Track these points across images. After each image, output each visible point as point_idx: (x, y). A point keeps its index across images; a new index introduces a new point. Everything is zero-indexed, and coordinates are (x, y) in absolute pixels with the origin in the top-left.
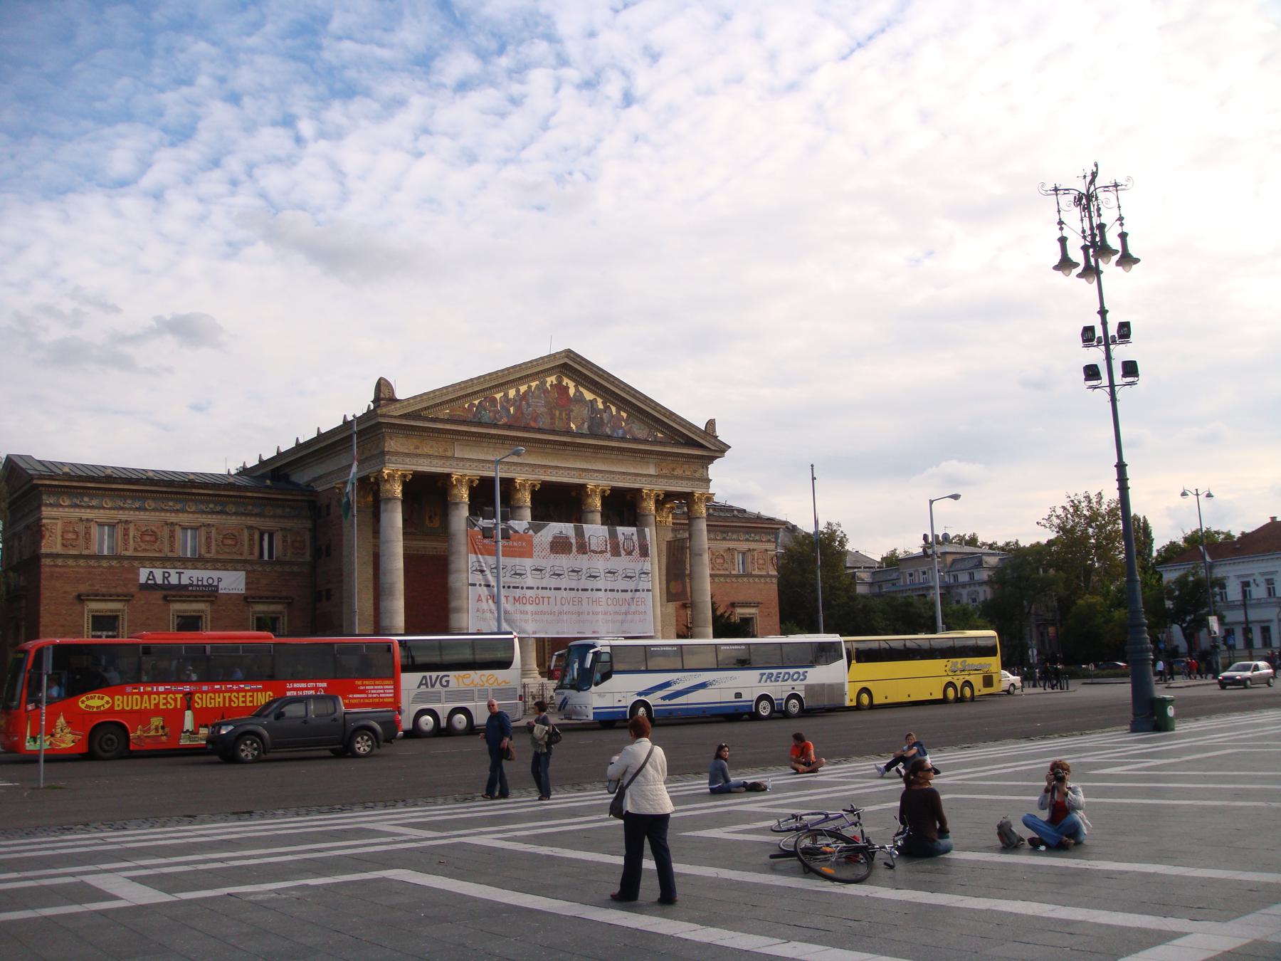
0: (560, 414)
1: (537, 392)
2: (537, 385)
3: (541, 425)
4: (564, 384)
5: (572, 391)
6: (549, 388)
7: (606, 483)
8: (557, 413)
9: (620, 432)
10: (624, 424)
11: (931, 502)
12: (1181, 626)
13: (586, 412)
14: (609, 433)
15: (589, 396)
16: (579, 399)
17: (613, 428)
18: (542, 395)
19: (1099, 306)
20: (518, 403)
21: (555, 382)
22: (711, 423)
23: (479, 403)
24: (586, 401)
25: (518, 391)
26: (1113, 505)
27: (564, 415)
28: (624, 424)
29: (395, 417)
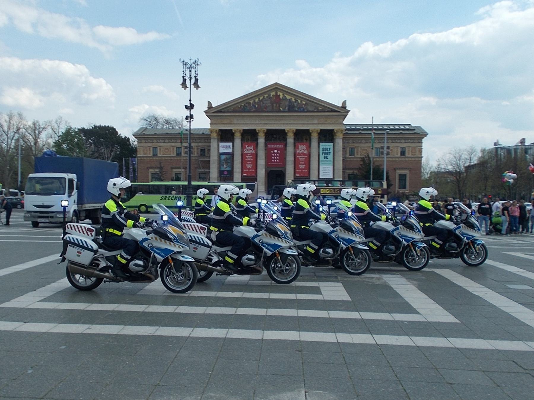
2: (267, 97)
3: (268, 110)
4: (278, 94)
5: (281, 97)
8: (275, 105)
9: (302, 109)
10: (303, 106)
13: (287, 103)
15: (288, 97)
16: (285, 99)
17: (298, 108)
18: (269, 99)
21: (274, 94)
22: (344, 103)
24: (287, 99)
25: (259, 99)
28: (303, 106)
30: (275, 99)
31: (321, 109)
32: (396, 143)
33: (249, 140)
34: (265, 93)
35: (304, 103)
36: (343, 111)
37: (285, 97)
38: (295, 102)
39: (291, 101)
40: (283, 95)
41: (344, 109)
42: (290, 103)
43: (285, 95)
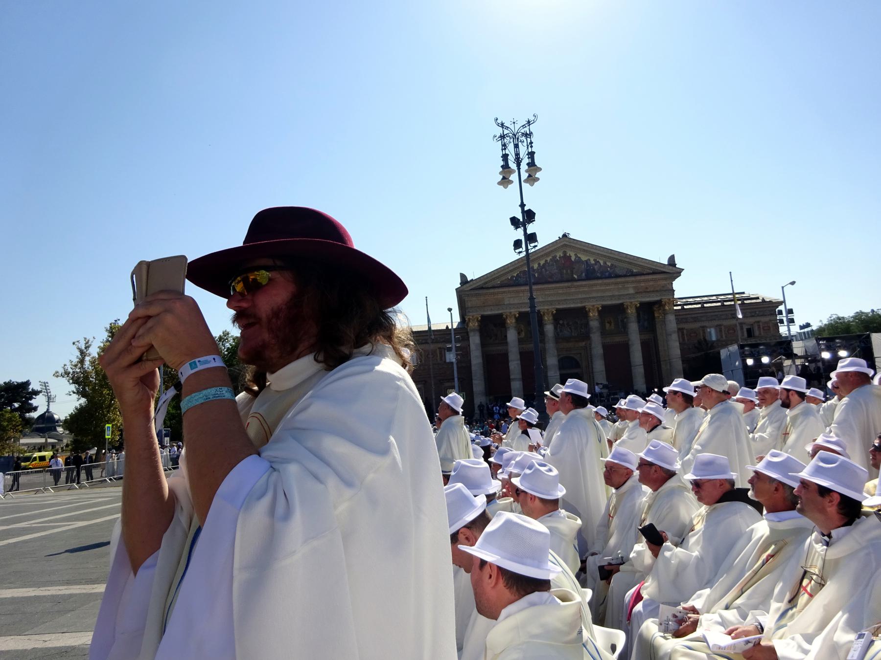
0: (567, 271)
1: (551, 263)
2: (550, 259)
4: (568, 255)
5: (573, 259)
6: (559, 259)
7: (599, 304)
8: (565, 271)
9: (607, 274)
10: (609, 269)
11: (783, 287)
12: (655, 392)
14: (600, 276)
16: (579, 261)
19: (520, 202)
20: (540, 271)
21: (562, 255)
22: (672, 259)
23: (517, 275)
27: (569, 271)
28: (609, 269)
29: (467, 291)
30: (563, 262)
31: (636, 272)
32: (758, 316)
33: (522, 331)
34: (547, 254)
35: (609, 264)
36: (671, 270)
37: (579, 257)
38: (596, 264)
39: (589, 263)
40: (576, 255)
41: (674, 268)
42: (587, 267)
43: (579, 255)
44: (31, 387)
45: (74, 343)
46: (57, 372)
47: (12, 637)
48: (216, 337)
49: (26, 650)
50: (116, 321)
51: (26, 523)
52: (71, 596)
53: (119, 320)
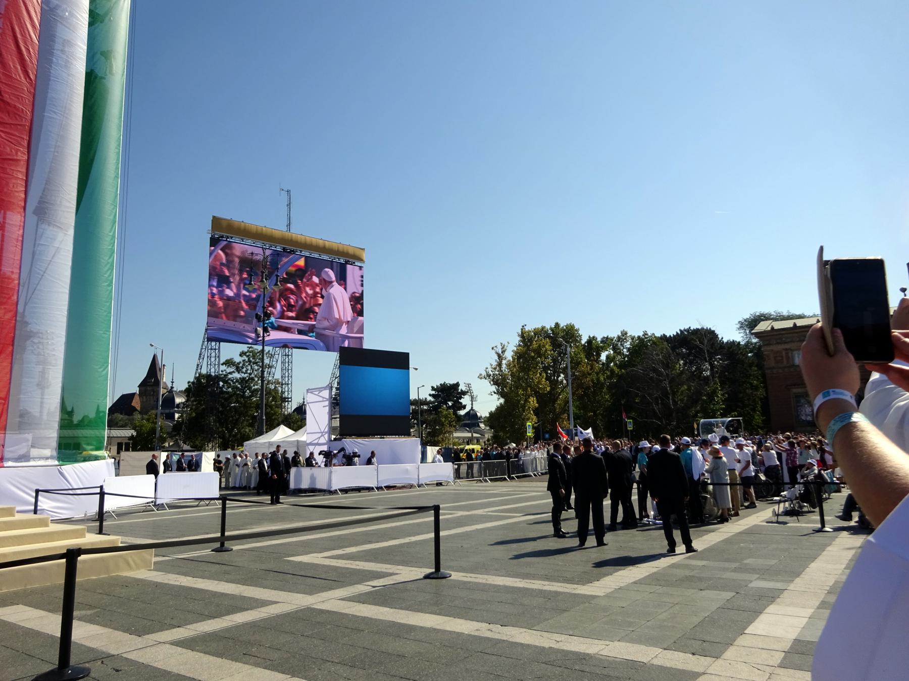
26: (466, 400)
44: (460, 388)
45: (493, 348)
46: (481, 375)
47: (525, 630)
48: (614, 337)
49: (544, 648)
50: (523, 326)
51: (482, 510)
52: (557, 593)
53: (526, 325)
